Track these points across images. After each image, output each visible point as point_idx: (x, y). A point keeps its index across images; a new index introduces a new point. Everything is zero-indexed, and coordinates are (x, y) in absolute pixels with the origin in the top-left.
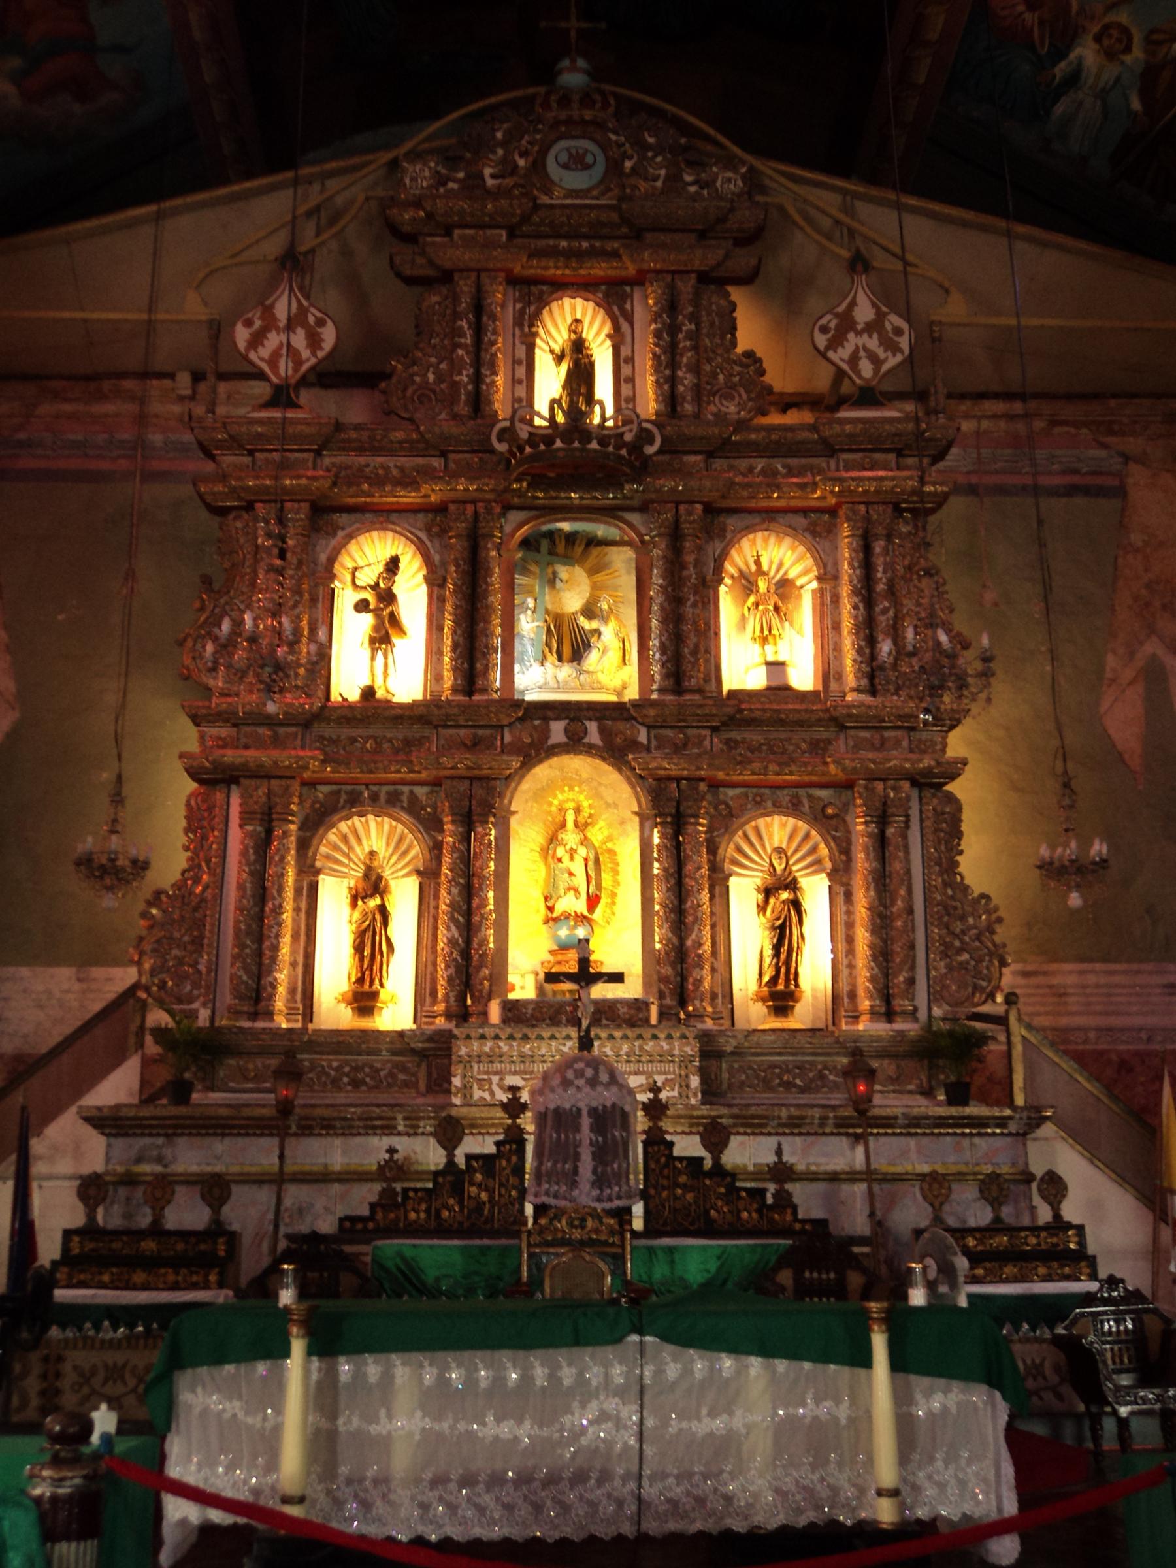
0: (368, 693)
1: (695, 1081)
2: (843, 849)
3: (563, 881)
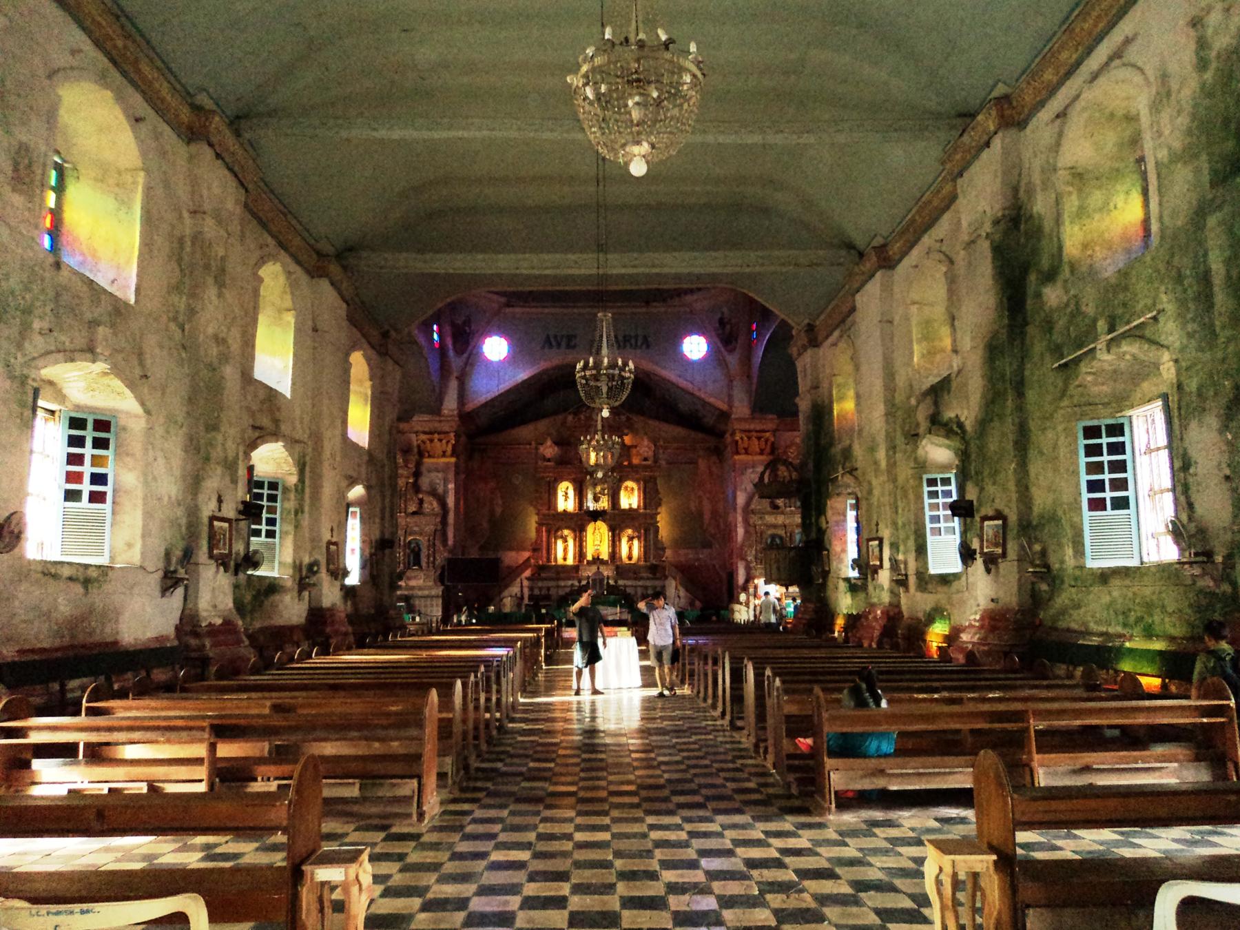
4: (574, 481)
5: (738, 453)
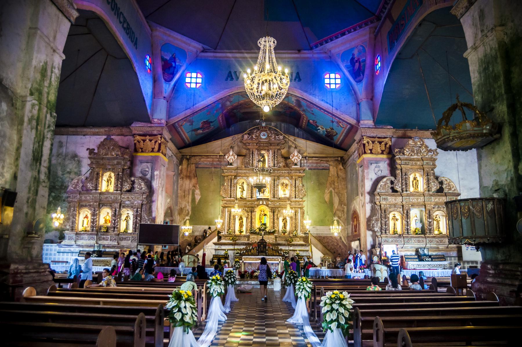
5: (365, 153)
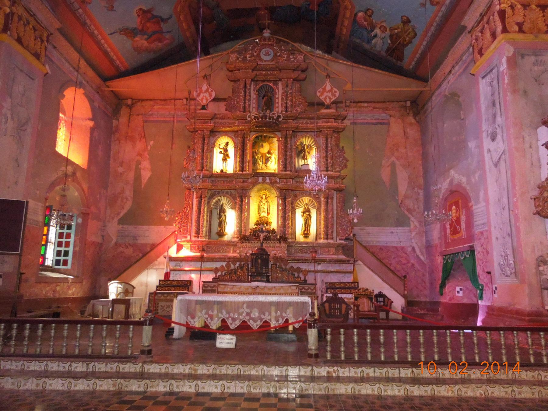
0: (222, 171)
1: (286, 252)
2: (319, 203)
3: (262, 209)
4: (234, 134)
